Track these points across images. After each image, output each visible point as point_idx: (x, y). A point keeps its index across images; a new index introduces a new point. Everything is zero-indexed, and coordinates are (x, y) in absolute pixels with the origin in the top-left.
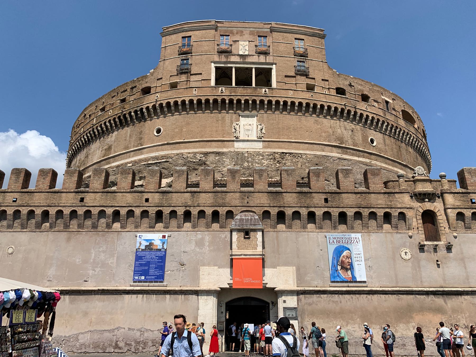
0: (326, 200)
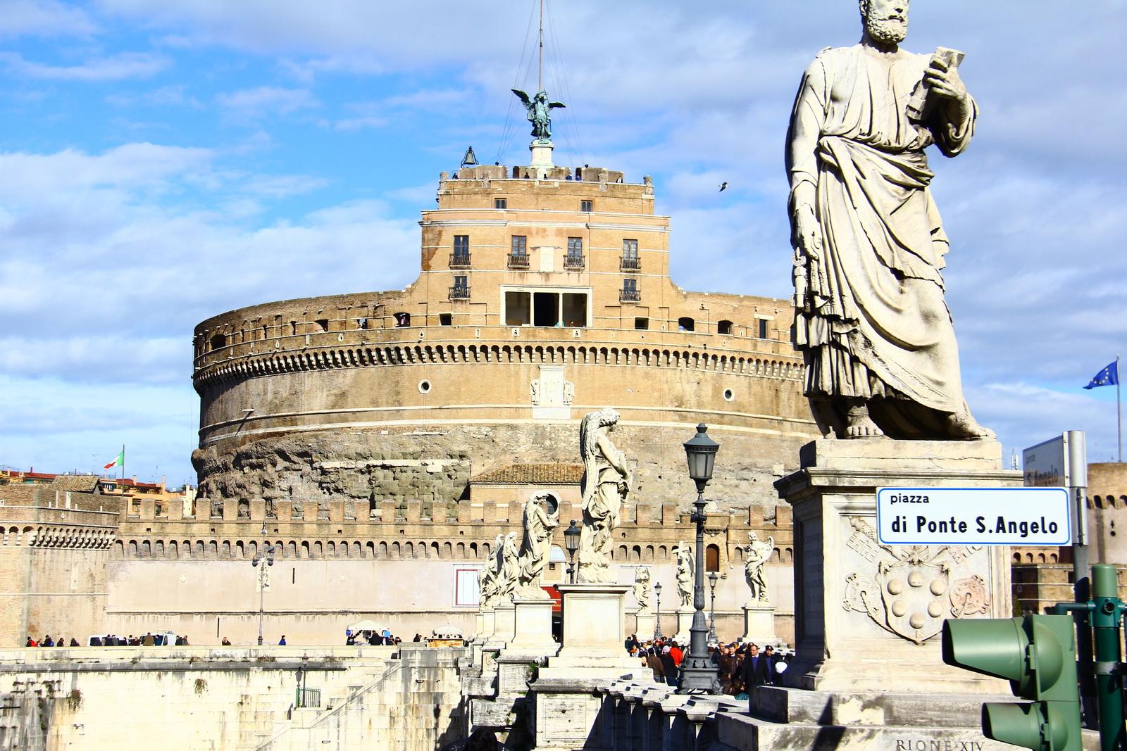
0: (623, 534)
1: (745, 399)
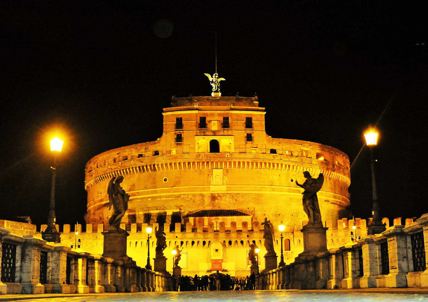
0: (248, 236)
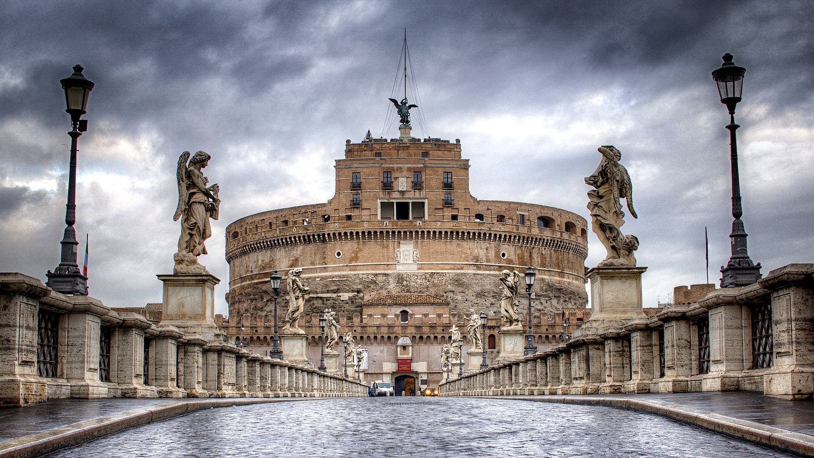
0: (443, 330)
1: (514, 257)
